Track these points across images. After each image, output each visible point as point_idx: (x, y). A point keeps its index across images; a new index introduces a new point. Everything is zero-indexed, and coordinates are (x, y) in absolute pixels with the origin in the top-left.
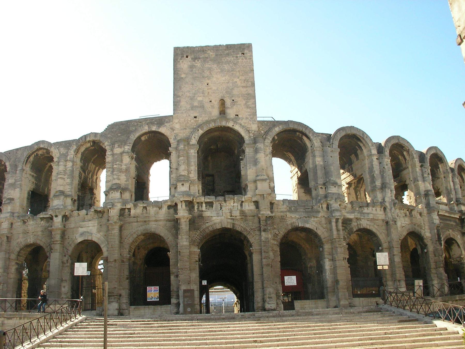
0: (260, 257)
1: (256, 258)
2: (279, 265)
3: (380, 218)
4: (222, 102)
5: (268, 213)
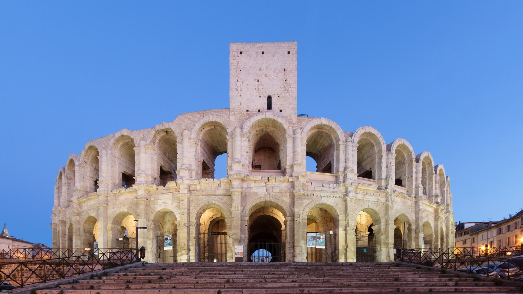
4: (269, 98)
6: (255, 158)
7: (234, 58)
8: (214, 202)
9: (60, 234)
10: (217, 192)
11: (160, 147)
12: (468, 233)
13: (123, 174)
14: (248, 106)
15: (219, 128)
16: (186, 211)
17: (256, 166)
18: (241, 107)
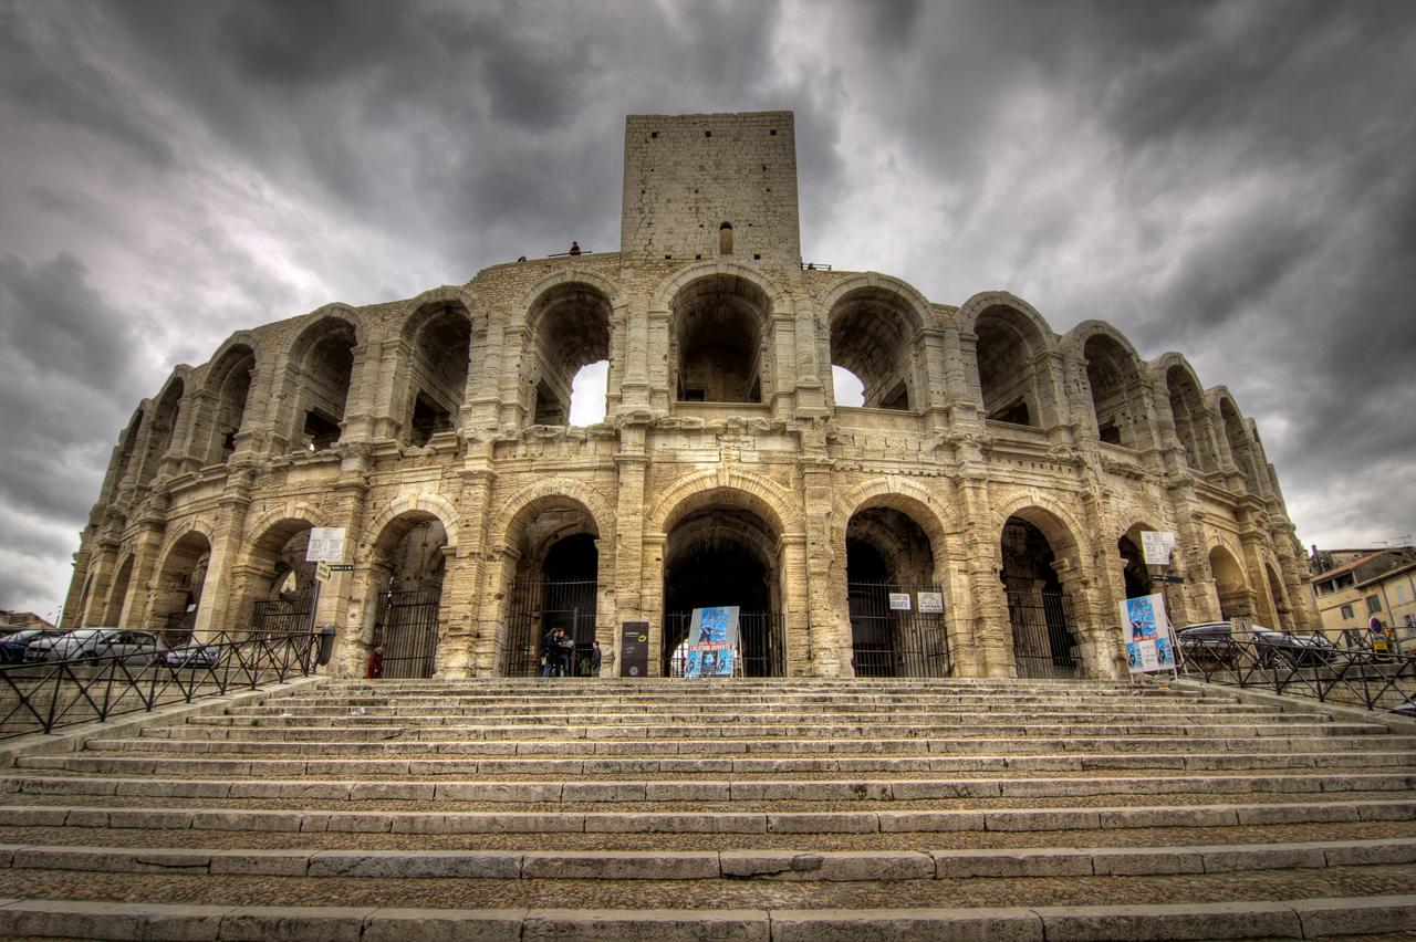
0: (802, 556)
1: (791, 556)
2: (843, 574)
3: (1070, 488)
5: (821, 457)
6: (689, 371)
7: (637, 145)
8: (563, 491)
9: (93, 586)
10: (575, 461)
11: (425, 346)
12: (1351, 582)
13: (309, 414)
14: (670, 248)
15: (589, 298)
16: (480, 515)
17: (689, 393)
18: (650, 248)
